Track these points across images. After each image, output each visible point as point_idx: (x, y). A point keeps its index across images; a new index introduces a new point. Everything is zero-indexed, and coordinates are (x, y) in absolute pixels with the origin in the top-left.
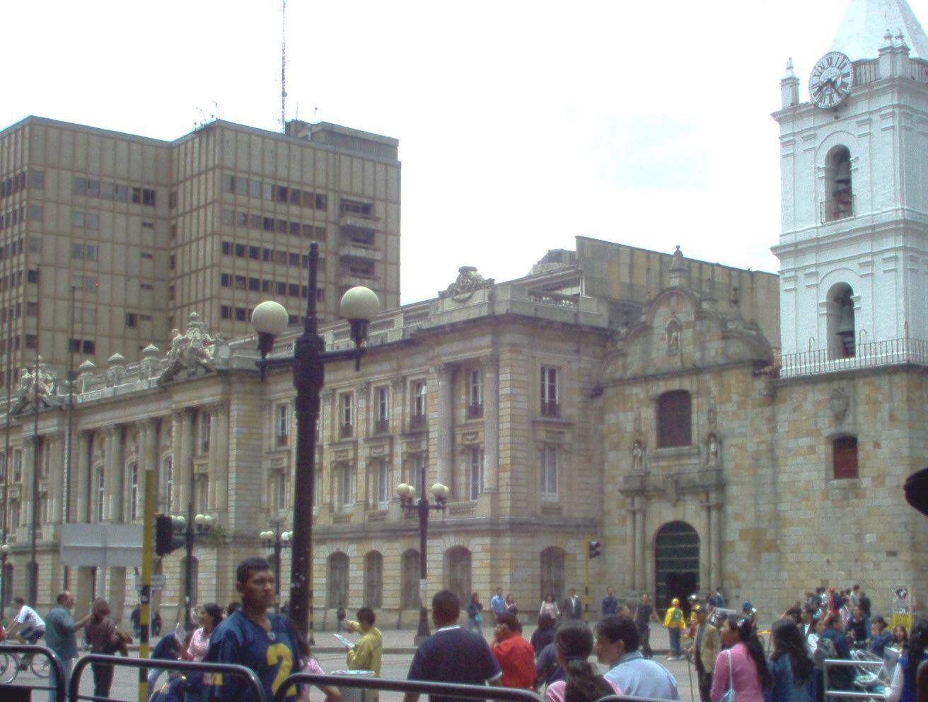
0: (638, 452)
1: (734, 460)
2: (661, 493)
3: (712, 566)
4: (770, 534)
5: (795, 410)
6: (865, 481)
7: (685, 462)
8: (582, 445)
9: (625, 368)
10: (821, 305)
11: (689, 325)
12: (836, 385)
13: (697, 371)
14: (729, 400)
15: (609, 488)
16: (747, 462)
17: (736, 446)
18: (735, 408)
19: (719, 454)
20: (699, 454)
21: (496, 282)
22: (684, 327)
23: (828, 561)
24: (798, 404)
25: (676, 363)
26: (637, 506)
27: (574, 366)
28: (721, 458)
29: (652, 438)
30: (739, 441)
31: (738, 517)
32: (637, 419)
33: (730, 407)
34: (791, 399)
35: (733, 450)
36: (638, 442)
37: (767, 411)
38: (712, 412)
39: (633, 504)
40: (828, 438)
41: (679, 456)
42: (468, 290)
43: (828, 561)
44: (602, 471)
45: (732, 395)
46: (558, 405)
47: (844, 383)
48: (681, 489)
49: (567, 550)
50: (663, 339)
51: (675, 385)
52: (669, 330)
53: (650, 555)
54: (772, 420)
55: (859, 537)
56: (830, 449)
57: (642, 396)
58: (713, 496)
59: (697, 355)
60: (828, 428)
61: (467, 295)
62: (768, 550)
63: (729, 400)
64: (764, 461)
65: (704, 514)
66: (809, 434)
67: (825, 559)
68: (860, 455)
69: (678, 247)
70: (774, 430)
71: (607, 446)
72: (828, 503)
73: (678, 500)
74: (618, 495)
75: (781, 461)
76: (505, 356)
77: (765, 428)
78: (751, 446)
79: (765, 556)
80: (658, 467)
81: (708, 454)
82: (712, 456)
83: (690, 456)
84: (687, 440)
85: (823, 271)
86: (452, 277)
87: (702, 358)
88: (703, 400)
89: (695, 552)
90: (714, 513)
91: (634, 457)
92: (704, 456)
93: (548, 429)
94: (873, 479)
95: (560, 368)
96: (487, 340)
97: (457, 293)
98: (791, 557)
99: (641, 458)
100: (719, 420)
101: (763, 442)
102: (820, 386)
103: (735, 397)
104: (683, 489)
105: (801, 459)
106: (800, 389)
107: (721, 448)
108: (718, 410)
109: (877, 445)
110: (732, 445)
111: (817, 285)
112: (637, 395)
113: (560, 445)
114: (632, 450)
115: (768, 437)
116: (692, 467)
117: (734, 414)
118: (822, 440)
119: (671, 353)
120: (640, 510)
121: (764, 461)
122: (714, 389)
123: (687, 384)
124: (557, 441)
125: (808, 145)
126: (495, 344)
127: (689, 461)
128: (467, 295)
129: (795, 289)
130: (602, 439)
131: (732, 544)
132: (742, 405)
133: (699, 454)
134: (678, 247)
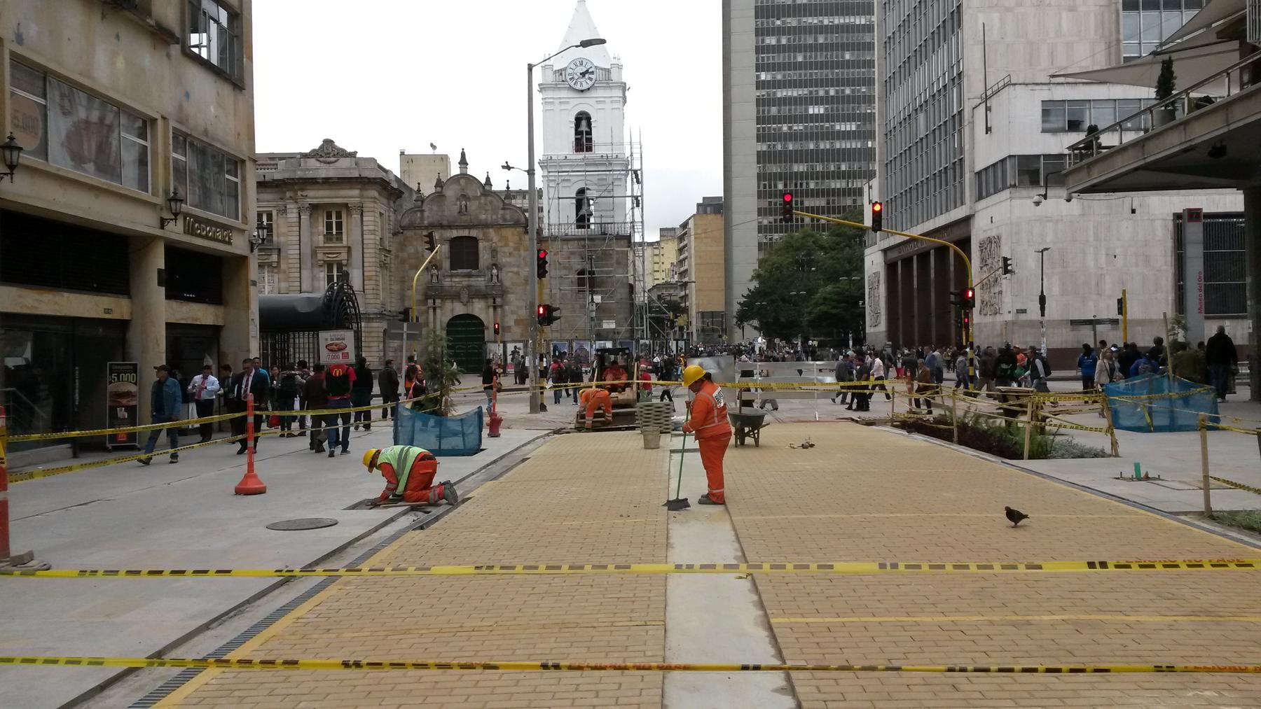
1: (508, 278)
2: (455, 297)
9: (422, 218)
11: (476, 198)
13: (485, 226)
14: (507, 245)
18: (511, 250)
20: (485, 276)
21: (358, 156)
29: (446, 264)
30: (515, 269)
31: (513, 312)
33: (506, 249)
35: (510, 274)
38: (494, 252)
41: (469, 276)
42: (334, 156)
48: (476, 294)
51: (465, 233)
52: (458, 199)
61: (333, 159)
63: (507, 245)
65: (491, 310)
76: (368, 205)
81: (492, 276)
83: (477, 276)
84: (475, 266)
86: (317, 144)
88: (486, 244)
89: (483, 332)
90: (499, 310)
91: (432, 276)
96: (356, 192)
97: (321, 156)
103: (511, 244)
116: (480, 282)
122: (495, 239)
123: (474, 233)
125: (563, 107)
126: (361, 196)
128: (333, 159)
132: (518, 249)
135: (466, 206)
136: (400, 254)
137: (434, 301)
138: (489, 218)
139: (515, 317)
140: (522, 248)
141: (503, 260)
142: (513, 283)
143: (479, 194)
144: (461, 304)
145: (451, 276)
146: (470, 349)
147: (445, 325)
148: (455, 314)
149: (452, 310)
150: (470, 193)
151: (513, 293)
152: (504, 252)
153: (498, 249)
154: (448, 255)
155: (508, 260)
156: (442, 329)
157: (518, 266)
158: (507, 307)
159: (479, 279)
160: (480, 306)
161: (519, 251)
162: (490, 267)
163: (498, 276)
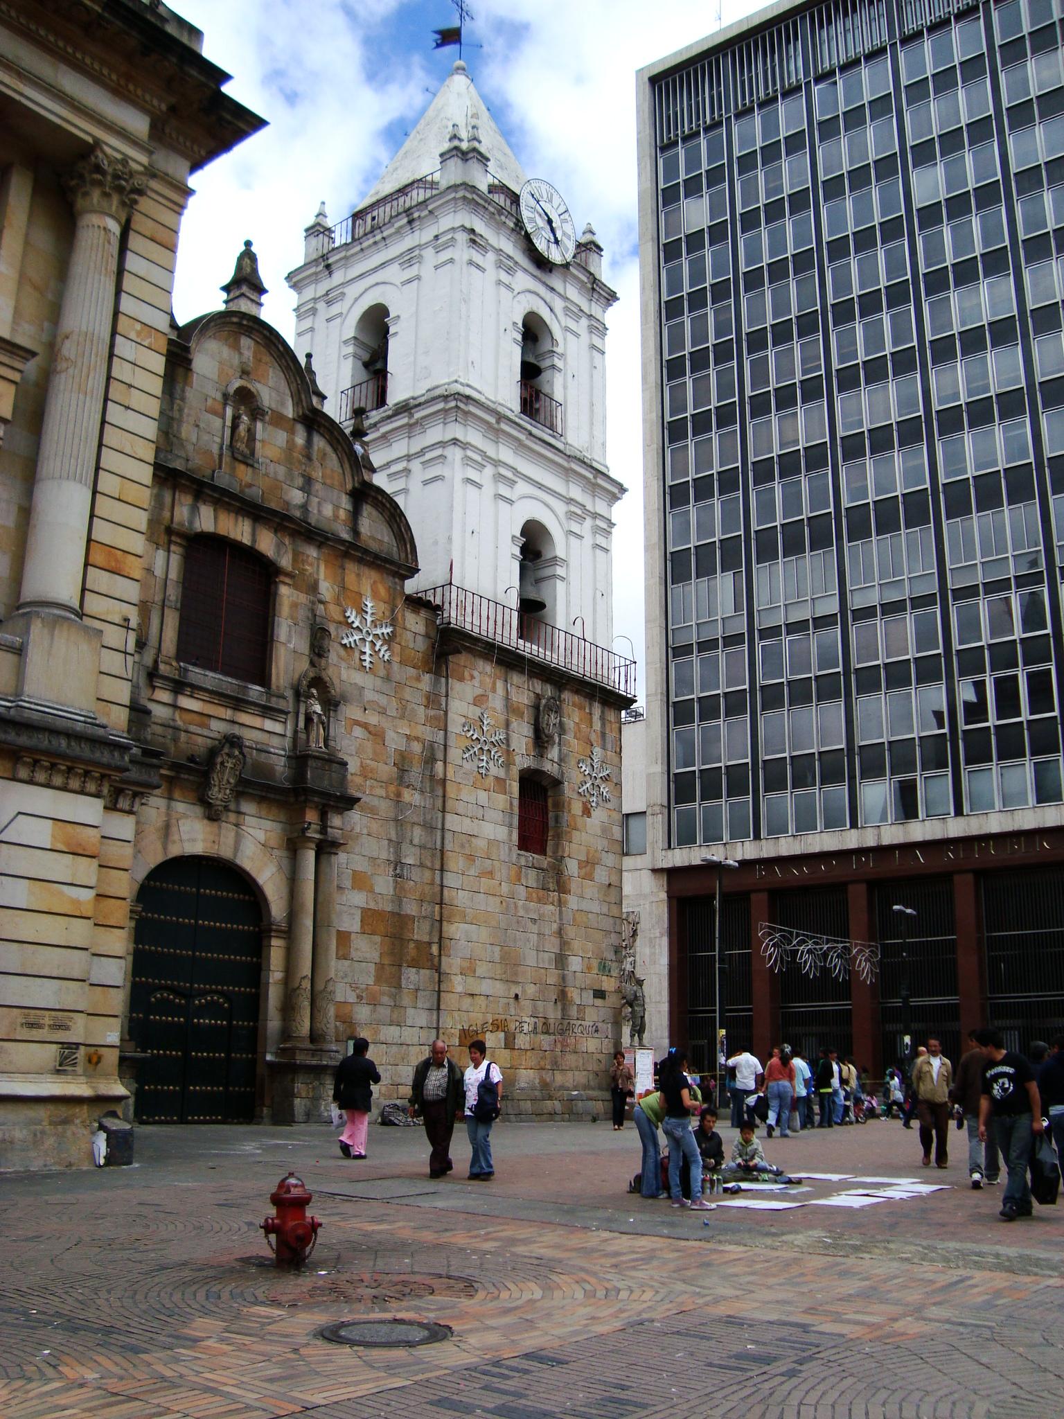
4: (421, 932)
6: (572, 867)
7: (244, 718)
16: (386, 770)
17: (365, 726)
23: (517, 996)
30: (373, 719)
31: (360, 881)
34: (472, 677)
35: (358, 732)
41: (238, 703)
43: (517, 996)
54: (432, 700)
55: (561, 960)
60: (523, 759)
62: (415, 964)
64: (415, 773)
68: (566, 817)
69: (248, 244)
78: (394, 741)
79: (412, 976)
80: (174, 706)
85: (522, 488)
87: (304, 507)
88: (303, 598)
94: (581, 864)
98: (458, 984)
100: (333, 657)
102: (516, 678)
109: (587, 812)
110: (357, 723)
118: (515, 774)
121: (415, 773)
122: (326, 589)
123: (267, 543)
127: (256, 721)
134: (248, 244)
138: (313, 509)
139: (358, 899)
141: (342, 674)
142: (365, 772)
144: (198, 810)
145: (179, 686)
146: (201, 1011)
148: (175, 851)
149: (166, 830)
154: (174, 593)
155: (358, 678)
157: (383, 712)
159: (269, 725)
160: (261, 836)
162: (299, 695)
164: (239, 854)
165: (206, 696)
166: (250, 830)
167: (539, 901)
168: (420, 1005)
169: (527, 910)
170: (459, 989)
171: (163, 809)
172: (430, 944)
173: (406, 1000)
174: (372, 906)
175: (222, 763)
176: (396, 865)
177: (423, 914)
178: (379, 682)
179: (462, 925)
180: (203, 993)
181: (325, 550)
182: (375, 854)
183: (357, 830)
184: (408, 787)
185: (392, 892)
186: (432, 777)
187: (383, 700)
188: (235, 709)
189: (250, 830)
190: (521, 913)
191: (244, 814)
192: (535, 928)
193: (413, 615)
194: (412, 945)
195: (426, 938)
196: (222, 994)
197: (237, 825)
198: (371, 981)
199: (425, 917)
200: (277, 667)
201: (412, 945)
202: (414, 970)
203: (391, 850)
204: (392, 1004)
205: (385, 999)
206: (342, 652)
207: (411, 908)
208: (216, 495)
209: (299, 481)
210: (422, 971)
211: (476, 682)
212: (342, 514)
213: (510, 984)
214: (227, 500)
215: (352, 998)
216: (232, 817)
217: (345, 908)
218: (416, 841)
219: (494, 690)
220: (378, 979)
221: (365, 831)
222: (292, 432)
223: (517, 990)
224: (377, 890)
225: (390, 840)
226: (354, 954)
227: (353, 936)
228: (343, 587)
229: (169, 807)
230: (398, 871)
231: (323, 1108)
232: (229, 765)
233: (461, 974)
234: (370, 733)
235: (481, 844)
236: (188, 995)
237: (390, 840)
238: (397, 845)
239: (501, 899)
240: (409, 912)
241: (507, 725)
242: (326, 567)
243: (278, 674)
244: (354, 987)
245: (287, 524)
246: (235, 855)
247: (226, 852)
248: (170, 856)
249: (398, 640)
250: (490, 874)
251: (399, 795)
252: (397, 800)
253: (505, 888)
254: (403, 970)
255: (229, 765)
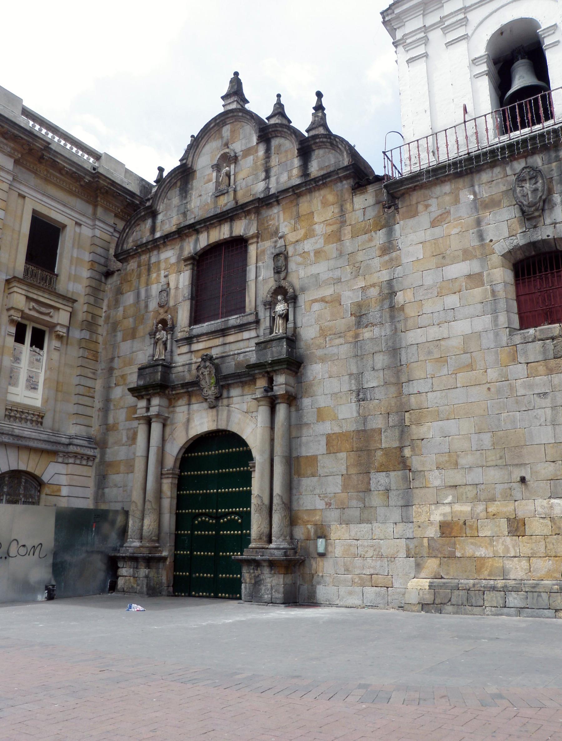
0: (162, 335)
3: (276, 501)
5: (434, 224)
7: (230, 339)
8: (86, 334)
9: (153, 230)
10: (475, 61)
12: (519, 165)
14: (309, 234)
15: (118, 392)
19: (291, 317)
22: (239, 158)
23: (523, 480)
24: (439, 212)
25: (226, 202)
26: (154, 410)
27: (86, 232)
28: (295, 323)
30: (328, 292)
32: (166, 290)
33: (308, 246)
34: (427, 206)
35: (316, 306)
36: (164, 322)
37: (380, 237)
39: (148, 409)
40: (508, 255)
41: (223, 332)
43: (523, 480)
44: (111, 370)
45: (316, 227)
46: (57, 275)
47: (538, 160)
49: (45, 478)
50: (210, 180)
52: (217, 167)
53: (168, 486)
56: (509, 276)
57: (173, 260)
58: (280, 380)
59: (261, 186)
62: (384, 469)
64: (374, 314)
65: (263, 412)
66: (467, 255)
67: (516, 476)
69: (236, 74)
70: (394, 264)
71: (119, 335)
72: (520, 370)
73: (218, 398)
74: (130, 399)
75: (410, 311)
77: (377, 262)
81: (273, 319)
82: (279, 322)
83: (241, 328)
87: (268, 188)
89: (247, 479)
90: (282, 410)
91: (156, 343)
92: (265, 323)
93: (31, 295)
95: (65, 226)
99: (165, 344)
101: (373, 285)
102: (485, 176)
103: (319, 229)
104: (226, 377)
105: (452, 300)
106: (447, 188)
107: (295, 308)
108: (291, 252)
111: (465, 37)
112: (167, 259)
113: (52, 326)
114: (153, 334)
115: (385, 276)
117: (318, 253)
118: (496, 259)
119: (219, 194)
120: (158, 415)
124: (47, 318)
127: (239, 336)
129: (426, 55)
130: (114, 327)
131: (313, 459)
133: (257, 322)
134: (236, 74)
135: (228, 175)
136: (113, 313)
137: (149, 401)
140: (347, 230)
142: (323, 333)
143: (255, 144)
145: (189, 340)
147: (170, 462)
150: (238, 147)
151: (323, 359)
152: (305, 254)
153: (290, 251)
155: (314, 269)
156: (161, 476)
157: (339, 281)
158: (306, 402)
159: (246, 335)
161: (340, 240)
162: (270, 305)
163: (285, 317)
164: (230, 424)
165: (205, 338)
166: (237, 406)
167: (550, 371)
168: (392, 503)
169: (530, 386)
170: (437, 483)
171: (186, 412)
172: (401, 448)
173: (376, 499)
174: (337, 430)
175: (202, 373)
176: (359, 391)
177: (391, 424)
178: (332, 262)
179: (435, 424)
180: (226, 515)
181: (284, 203)
182: (336, 390)
183: (320, 377)
184: (366, 327)
185: (355, 414)
186: (392, 308)
187: (338, 273)
188: (224, 336)
189: (237, 406)
190: (521, 392)
191: (232, 397)
192: (547, 402)
193: (362, 196)
194: (379, 453)
195: (396, 444)
196: (236, 513)
197: (228, 406)
198: (338, 489)
199: (392, 427)
200: (249, 296)
201: (379, 453)
202: (384, 474)
203: (353, 381)
204: (362, 505)
205: (354, 503)
206: (299, 259)
207: (377, 423)
208: (202, 225)
209: (263, 175)
210: (392, 474)
211: (433, 208)
212: (295, 172)
213: (510, 468)
214: (208, 223)
215: (320, 504)
216: (225, 402)
217: (311, 438)
218: (379, 366)
219: (457, 201)
220: (345, 487)
221: (327, 376)
222: (257, 152)
223: (517, 474)
224: (341, 416)
225: (351, 375)
226: (321, 471)
227: (319, 458)
228: (298, 217)
229: (189, 410)
230: (361, 396)
231: (263, 591)
232: (206, 373)
233: (438, 468)
234: (327, 302)
235: (455, 343)
236: (218, 517)
237: (351, 375)
238: (359, 376)
239: (488, 385)
240: (374, 426)
241: (478, 222)
242: (284, 213)
243: (250, 301)
244: (322, 496)
245: (247, 209)
246: (227, 425)
247: (222, 426)
248: (190, 437)
249: (348, 223)
250: (471, 367)
251: (357, 336)
252: (357, 341)
253: (493, 374)
254: (372, 475)
255: (206, 373)
